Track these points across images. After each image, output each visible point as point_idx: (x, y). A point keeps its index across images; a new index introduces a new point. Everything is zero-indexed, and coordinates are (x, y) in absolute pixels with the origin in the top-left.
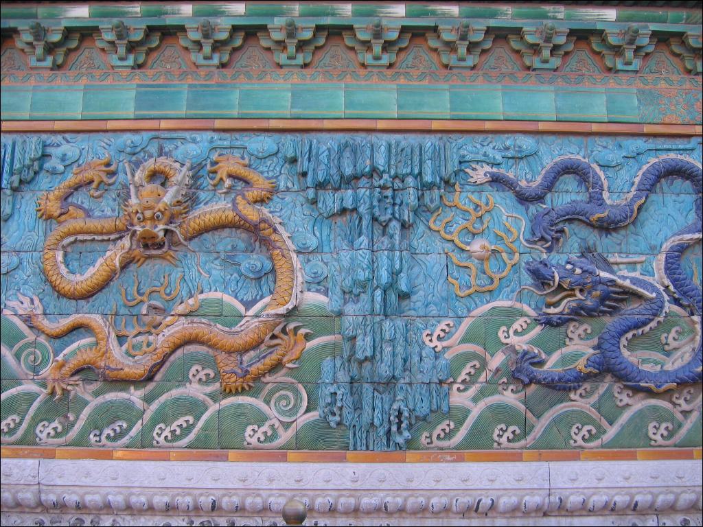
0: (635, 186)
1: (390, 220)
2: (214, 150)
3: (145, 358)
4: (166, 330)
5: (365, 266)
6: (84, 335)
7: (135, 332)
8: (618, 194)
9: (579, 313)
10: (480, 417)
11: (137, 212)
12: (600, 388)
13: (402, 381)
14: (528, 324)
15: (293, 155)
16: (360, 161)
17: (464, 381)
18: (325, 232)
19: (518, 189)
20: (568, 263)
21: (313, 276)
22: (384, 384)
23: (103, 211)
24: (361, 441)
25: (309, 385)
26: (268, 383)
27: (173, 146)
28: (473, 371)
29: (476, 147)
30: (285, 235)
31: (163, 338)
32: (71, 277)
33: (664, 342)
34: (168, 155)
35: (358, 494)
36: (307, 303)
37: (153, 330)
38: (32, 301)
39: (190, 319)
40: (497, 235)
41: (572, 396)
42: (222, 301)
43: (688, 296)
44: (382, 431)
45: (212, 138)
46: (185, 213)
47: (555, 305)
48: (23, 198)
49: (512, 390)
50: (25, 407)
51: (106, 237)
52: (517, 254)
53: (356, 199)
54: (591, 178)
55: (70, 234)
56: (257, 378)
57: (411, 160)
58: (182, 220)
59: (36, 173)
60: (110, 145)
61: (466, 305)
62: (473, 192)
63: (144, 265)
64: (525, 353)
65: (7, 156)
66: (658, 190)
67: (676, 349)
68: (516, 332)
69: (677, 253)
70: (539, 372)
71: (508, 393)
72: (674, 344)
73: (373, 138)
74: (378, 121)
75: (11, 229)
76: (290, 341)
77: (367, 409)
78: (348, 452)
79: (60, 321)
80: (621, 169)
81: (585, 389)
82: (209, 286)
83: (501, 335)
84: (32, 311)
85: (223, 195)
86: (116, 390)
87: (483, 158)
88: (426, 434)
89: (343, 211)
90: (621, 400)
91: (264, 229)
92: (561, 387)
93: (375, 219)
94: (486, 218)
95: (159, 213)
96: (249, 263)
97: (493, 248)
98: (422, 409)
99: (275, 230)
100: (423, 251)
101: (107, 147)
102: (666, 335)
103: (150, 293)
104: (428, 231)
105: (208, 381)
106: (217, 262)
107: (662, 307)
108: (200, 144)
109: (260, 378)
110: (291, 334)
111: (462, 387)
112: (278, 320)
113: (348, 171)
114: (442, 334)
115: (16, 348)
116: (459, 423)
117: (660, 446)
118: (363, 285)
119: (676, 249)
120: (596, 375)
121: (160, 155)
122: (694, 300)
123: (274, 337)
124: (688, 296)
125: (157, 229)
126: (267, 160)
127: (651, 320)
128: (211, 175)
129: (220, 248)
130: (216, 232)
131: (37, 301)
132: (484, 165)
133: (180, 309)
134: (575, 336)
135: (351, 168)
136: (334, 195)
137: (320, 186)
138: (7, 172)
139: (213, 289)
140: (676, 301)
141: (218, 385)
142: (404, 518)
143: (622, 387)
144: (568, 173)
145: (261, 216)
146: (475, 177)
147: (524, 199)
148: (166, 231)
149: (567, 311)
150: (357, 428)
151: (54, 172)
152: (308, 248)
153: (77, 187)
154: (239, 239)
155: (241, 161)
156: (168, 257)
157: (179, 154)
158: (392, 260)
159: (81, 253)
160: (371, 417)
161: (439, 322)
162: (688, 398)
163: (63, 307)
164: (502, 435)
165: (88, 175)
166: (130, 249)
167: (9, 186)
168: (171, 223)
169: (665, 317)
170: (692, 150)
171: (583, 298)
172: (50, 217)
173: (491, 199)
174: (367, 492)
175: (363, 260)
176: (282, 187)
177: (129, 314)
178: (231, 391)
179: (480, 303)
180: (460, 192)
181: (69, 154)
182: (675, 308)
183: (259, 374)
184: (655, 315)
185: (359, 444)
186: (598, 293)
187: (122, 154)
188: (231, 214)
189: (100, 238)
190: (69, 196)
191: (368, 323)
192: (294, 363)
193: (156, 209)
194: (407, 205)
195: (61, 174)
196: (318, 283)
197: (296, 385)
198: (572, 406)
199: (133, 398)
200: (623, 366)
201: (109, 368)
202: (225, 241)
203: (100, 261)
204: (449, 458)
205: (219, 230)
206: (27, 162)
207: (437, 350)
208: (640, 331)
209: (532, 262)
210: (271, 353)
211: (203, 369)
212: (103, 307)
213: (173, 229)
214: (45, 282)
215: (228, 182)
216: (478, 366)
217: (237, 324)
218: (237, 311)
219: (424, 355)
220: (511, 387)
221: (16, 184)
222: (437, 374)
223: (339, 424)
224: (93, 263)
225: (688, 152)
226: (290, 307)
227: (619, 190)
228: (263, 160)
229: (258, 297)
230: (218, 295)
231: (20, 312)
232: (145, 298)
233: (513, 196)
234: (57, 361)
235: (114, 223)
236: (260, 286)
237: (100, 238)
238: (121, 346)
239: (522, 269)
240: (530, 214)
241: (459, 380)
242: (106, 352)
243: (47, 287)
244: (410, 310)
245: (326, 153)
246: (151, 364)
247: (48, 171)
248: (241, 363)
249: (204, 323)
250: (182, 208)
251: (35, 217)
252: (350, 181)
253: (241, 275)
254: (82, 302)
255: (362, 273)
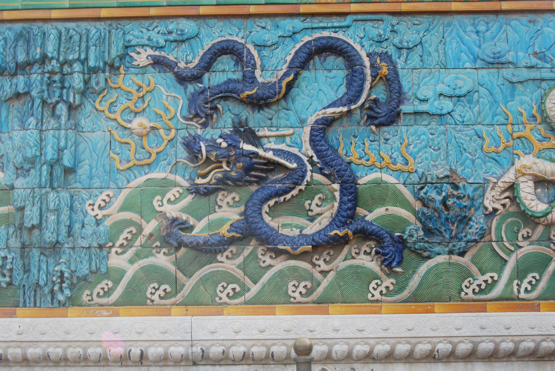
0: (287, 64)
1: (58, 102)
5: (32, 144)
8: (272, 72)
9: (225, 184)
10: (134, 277)
12: (245, 251)
13: (66, 245)
14: (180, 194)
16: (33, 49)
17: (121, 246)
19: (176, 70)
20: (221, 137)
22: (49, 248)
24: (30, 299)
28: (130, 236)
29: (142, 32)
33: (308, 207)
35: (24, 345)
40: (157, 114)
41: (219, 257)
43: (329, 165)
44: (47, 290)
47: (204, 176)
49: (164, 253)
52: (173, 131)
53: (28, 85)
54: (245, 58)
57: (80, 46)
61: (126, 178)
62: (137, 74)
64: (174, 220)
66: (311, 67)
67: (319, 215)
68: (169, 200)
69: (320, 126)
70: (186, 237)
71: (161, 256)
72: (317, 210)
73: (47, 27)
74: (53, 11)
77: (34, 270)
78: (18, 308)
80: (277, 48)
81: (231, 252)
83: (155, 204)
87: (147, 42)
88: (87, 292)
89: (18, 96)
90: (264, 262)
92: (209, 250)
93: (44, 102)
94: (148, 98)
97: (152, 125)
98: (84, 270)
100: (89, 129)
102: (309, 202)
104: (95, 111)
107: (303, 177)
111: (120, 251)
113: (21, 58)
114: (103, 204)
116: (117, 282)
117: (299, 303)
118: (32, 161)
119: (320, 122)
120: (239, 239)
122: (334, 169)
124: (329, 165)
127: (293, 188)
132: (147, 48)
134: (224, 204)
135: (24, 56)
140: (321, 171)
142: (69, 366)
143: (266, 249)
144: (226, 54)
146: (139, 60)
147: (183, 79)
149: (214, 181)
150: (27, 287)
158: (58, 139)
160: (36, 278)
161: (101, 193)
162: (328, 259)
164: (154, 292)
169: (307, 185)
170: (348, 27)
171: (228, 169)
173: (152, 80)
174: (31, 343)
175: (31, 139)
179: (139, 175)
180: (125, 74)
182: (318, 177)
184: (296, 184)
185: (28, 301)
186: (241, 164)
191: (35, 195)
194: (73, 87)
198: (218, 267)
200: (263, 230)
204: (105, 313)
207: (98, 218)
208: (282, 199)
209: (187, 137)
216: (134, 231)
219: (86, 223)
220: (164, 250)
222: (97, 239)
223: (10, 284)
225: (344, 29)
227: (273, 68)
233: (173, 77)
239: (178, 144)
240: (188, 93)
241: (117, 244)
244: (76, 182)
252: (23, 68)
255: (29, 151)
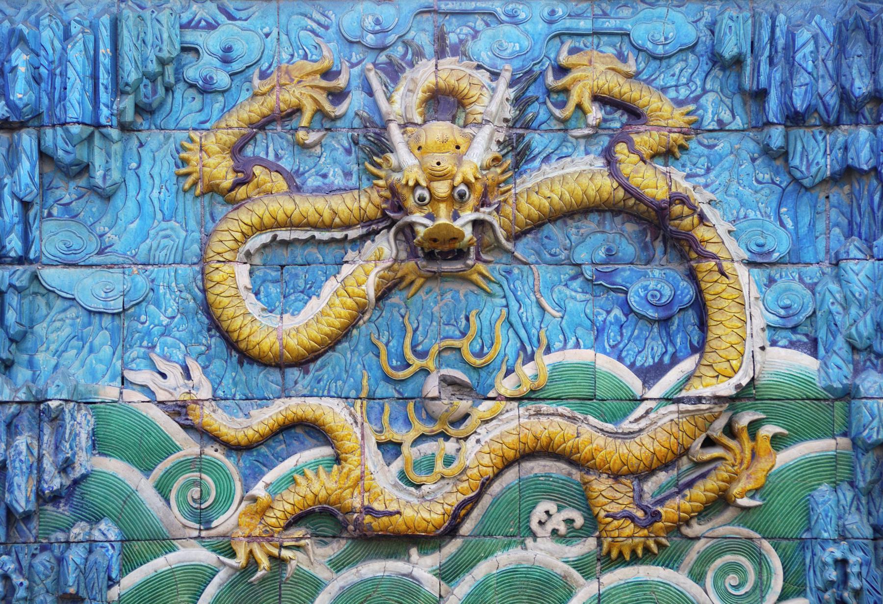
2: (557, 41)
3: (439, 489)
4: (482, 430)
6: (302, 443)
7: (413, 434)
11: (417, 184)
15: (736, 50)
18: (805, 220)
21: (782, 312)
23: (325, 176)
25: (784, 543)
26: (698, 538)
27: (466, 30)
30: (722, 227)
31: (478, 447)
32: (273, 320)
34: (458, 50)
36: (772, 371)
37: (451, 431)
38: (187, 373)
39: (532, 406)
42: (595, 368)
45: (553, 12)
46: (506, 182)
48: (141, 145)
50: (186, 597)
51: (338, 235)
55: (262, 228)
56: (676, 528)
58: (502, 199)
59: (168, 89)
60: (327, 28)
63: (422, 293)
65: (102, 50)
75: (121, 215)
76: (742, 451)
79: (253, 412)
82: (561, 337)
84: (189, 393)
85: (582, 141)
86: (378, 556)
91: (681, 217)
95: (463, 187)
96: (645, 288)
99: (702, 218)
101: (320, 30)
103: (440, 352)
105: (572, 534)
106: (576, 284)
108: (528, 26)
109: (679, 528)
110: (745, 436)
112: (717, 409)
115: (159, 471)
121: (440, 53)
123: (709, 443)
125: (457, 224)
126: (673, 60)
128: (555, 96)
129: (582, 255)
130: (569, 222)
131: (196, 372)
133: (506, 386)
136: (825, 137)
137: (794, 119)
138: (106, 88)
139: (572, 341)
141: (591, 542)
145: (673, 190)
148: (476, 223)
151: (205, 89)
152: (770, 253)
153: (264, 124)
154: (624, 239)
155: (620, 66)
156: (476, 277)
157: (481, 49)
159: (282, 267)
163: (254, 383)
165: (290, 96)
166: (395, 260)
167: (115, 123)
168: (482, 206)
172: (212, 190)
176: (709, 123)
177: (396, 395)
178: (621, 554)
181: (239, 48)
183: (680, 519)
187: (356, 48)
188: (604, 185)
189: (325, 236)
190: (247, 143)
192: (752, 497)
193: (459, 179)
195: (223, 92)
196: (794, 329)
197: (757, 543)
199: (418, 572)
201: (369, 510)
202: (591, 243)
203: (330, 286)
205: (576, 217)
206: (153, 67)
210: (703, 476)
211: (560, 509)
212: (340, 383)
213: (488, 218)
214: (209, 330)
215: (595, 114)
217: (625, 416)
218: (621, 386)
221: (129, 116)
224: (310, 291)
226: (744, 382)
228: (664, 63)
229: (667, 359)
230: (585, 355)
231: (162, 396)
232: (430, 363)
234: (255, 499)
235: (356, 205)
236: (668, 334)
237: (325, 236)
238: (389, 465)
242: (362, 478)
243: (215, 341)
245: (810, 47)
246: (455, 499)
247: (191, 86)
248: (641, 496)
249: (562, 415)
250: (499, 170)
251: (174, 188)
253: (628, 310)
254: (294, 373)
